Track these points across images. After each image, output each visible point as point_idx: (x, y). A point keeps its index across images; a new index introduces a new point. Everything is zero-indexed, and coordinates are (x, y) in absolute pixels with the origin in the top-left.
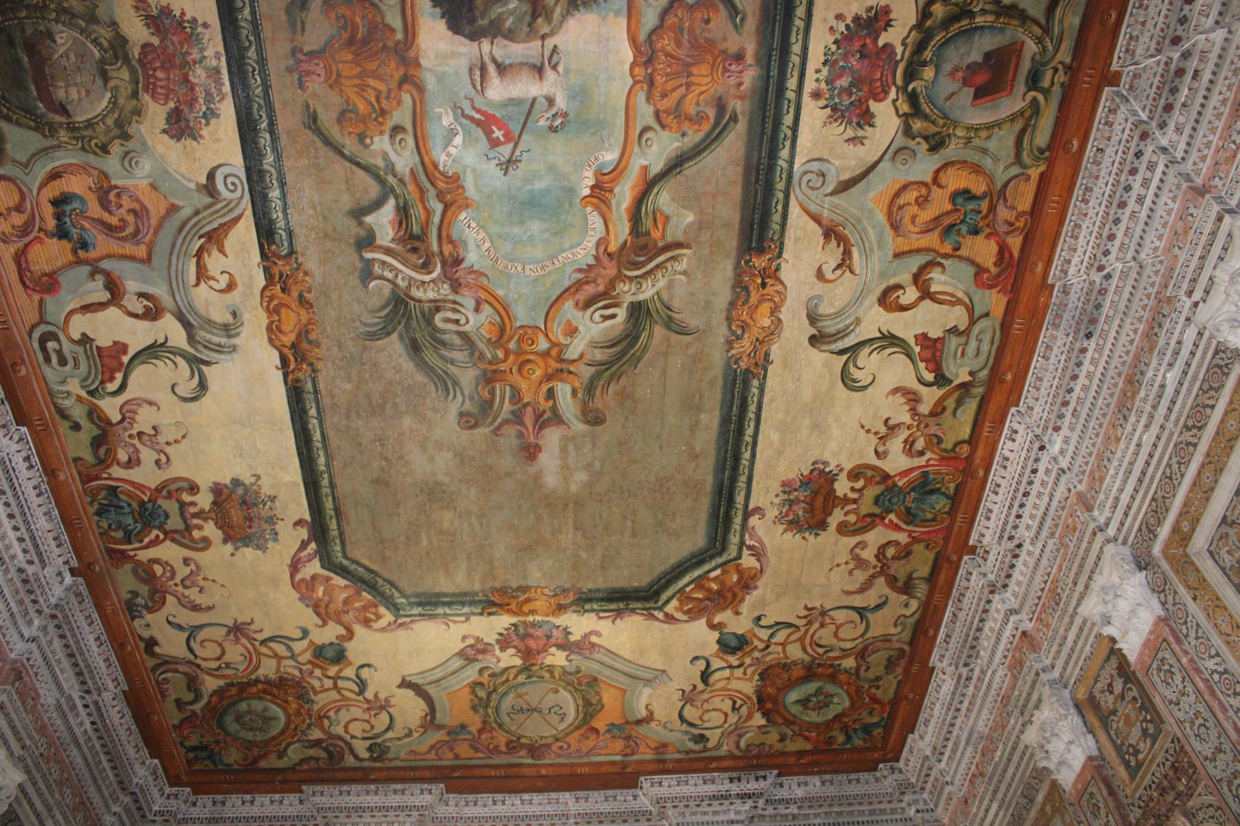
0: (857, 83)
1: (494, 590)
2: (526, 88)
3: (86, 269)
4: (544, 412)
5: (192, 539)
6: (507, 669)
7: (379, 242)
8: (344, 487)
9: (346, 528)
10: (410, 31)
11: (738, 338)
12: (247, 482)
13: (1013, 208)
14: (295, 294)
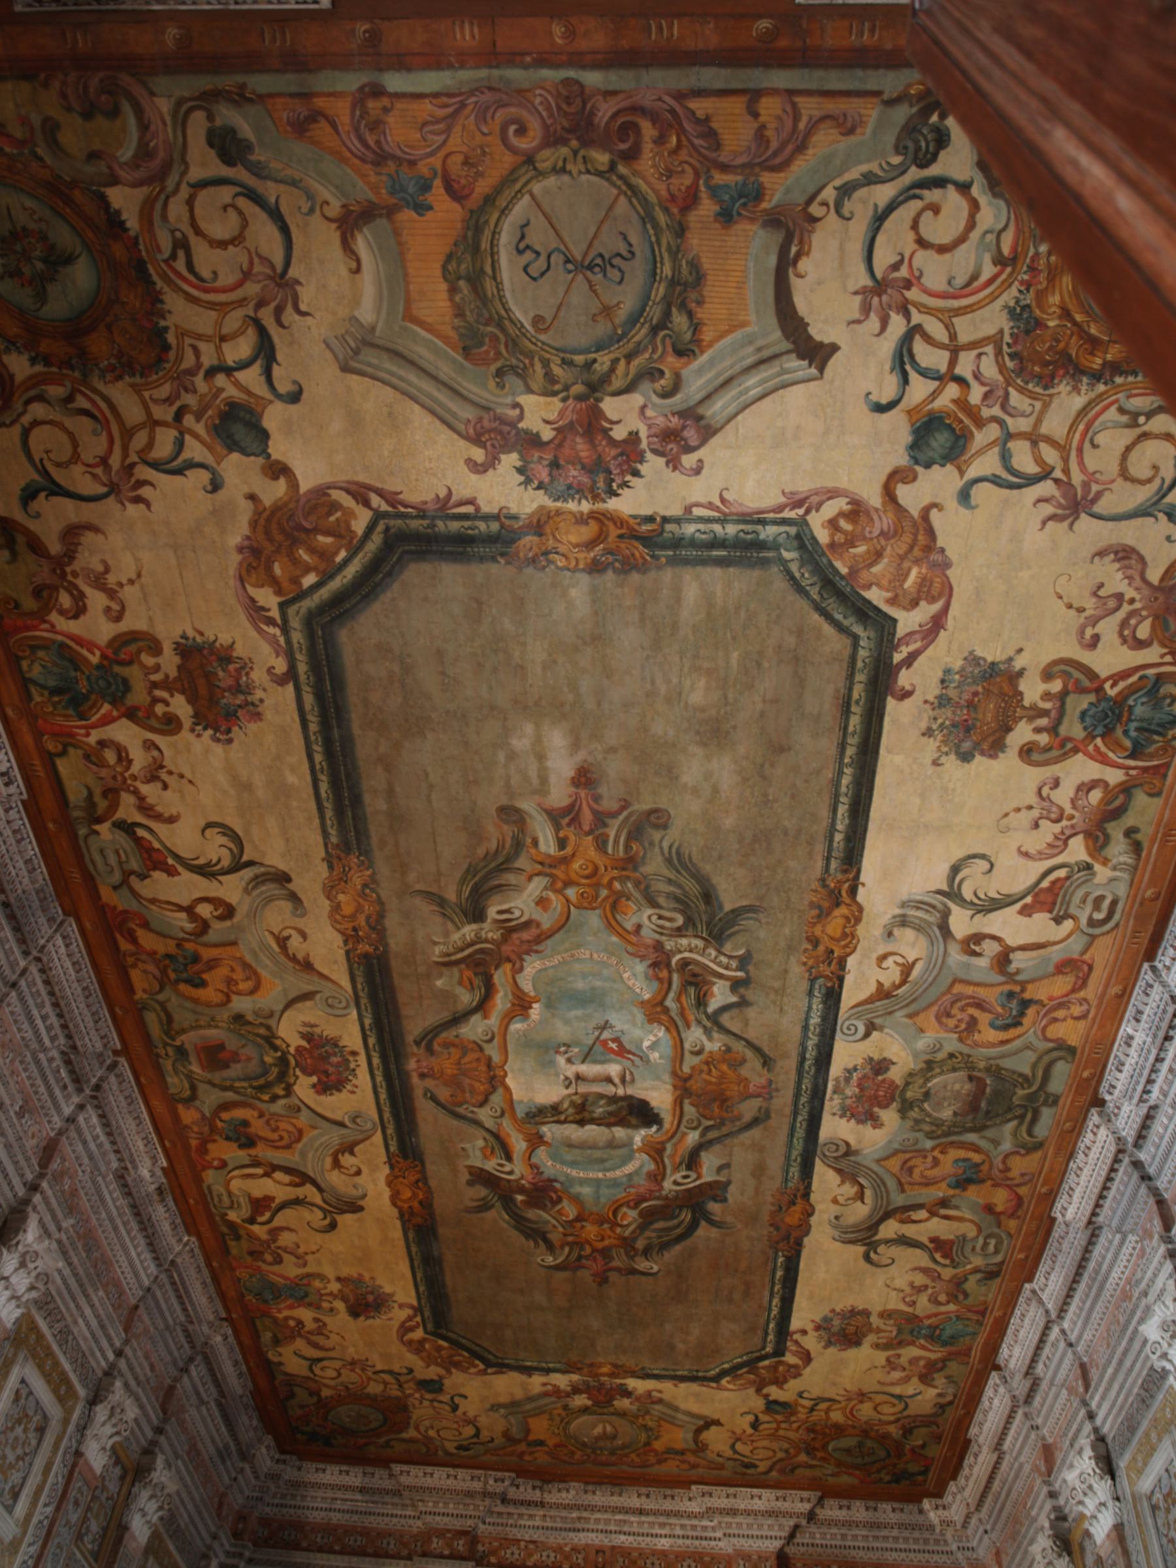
0: (324, 1058)
1: (642, 568)
3: (1019, 978)
4: (569, 825)
5: (1066, 675)
6: (629, 389)
7: (728, 984)
8: (828, 745)
9: (841, 684)
10: (678, 1103)
11: (365, 886)
12: (953, 757)
13: (145, 971)
14: (821, 948)
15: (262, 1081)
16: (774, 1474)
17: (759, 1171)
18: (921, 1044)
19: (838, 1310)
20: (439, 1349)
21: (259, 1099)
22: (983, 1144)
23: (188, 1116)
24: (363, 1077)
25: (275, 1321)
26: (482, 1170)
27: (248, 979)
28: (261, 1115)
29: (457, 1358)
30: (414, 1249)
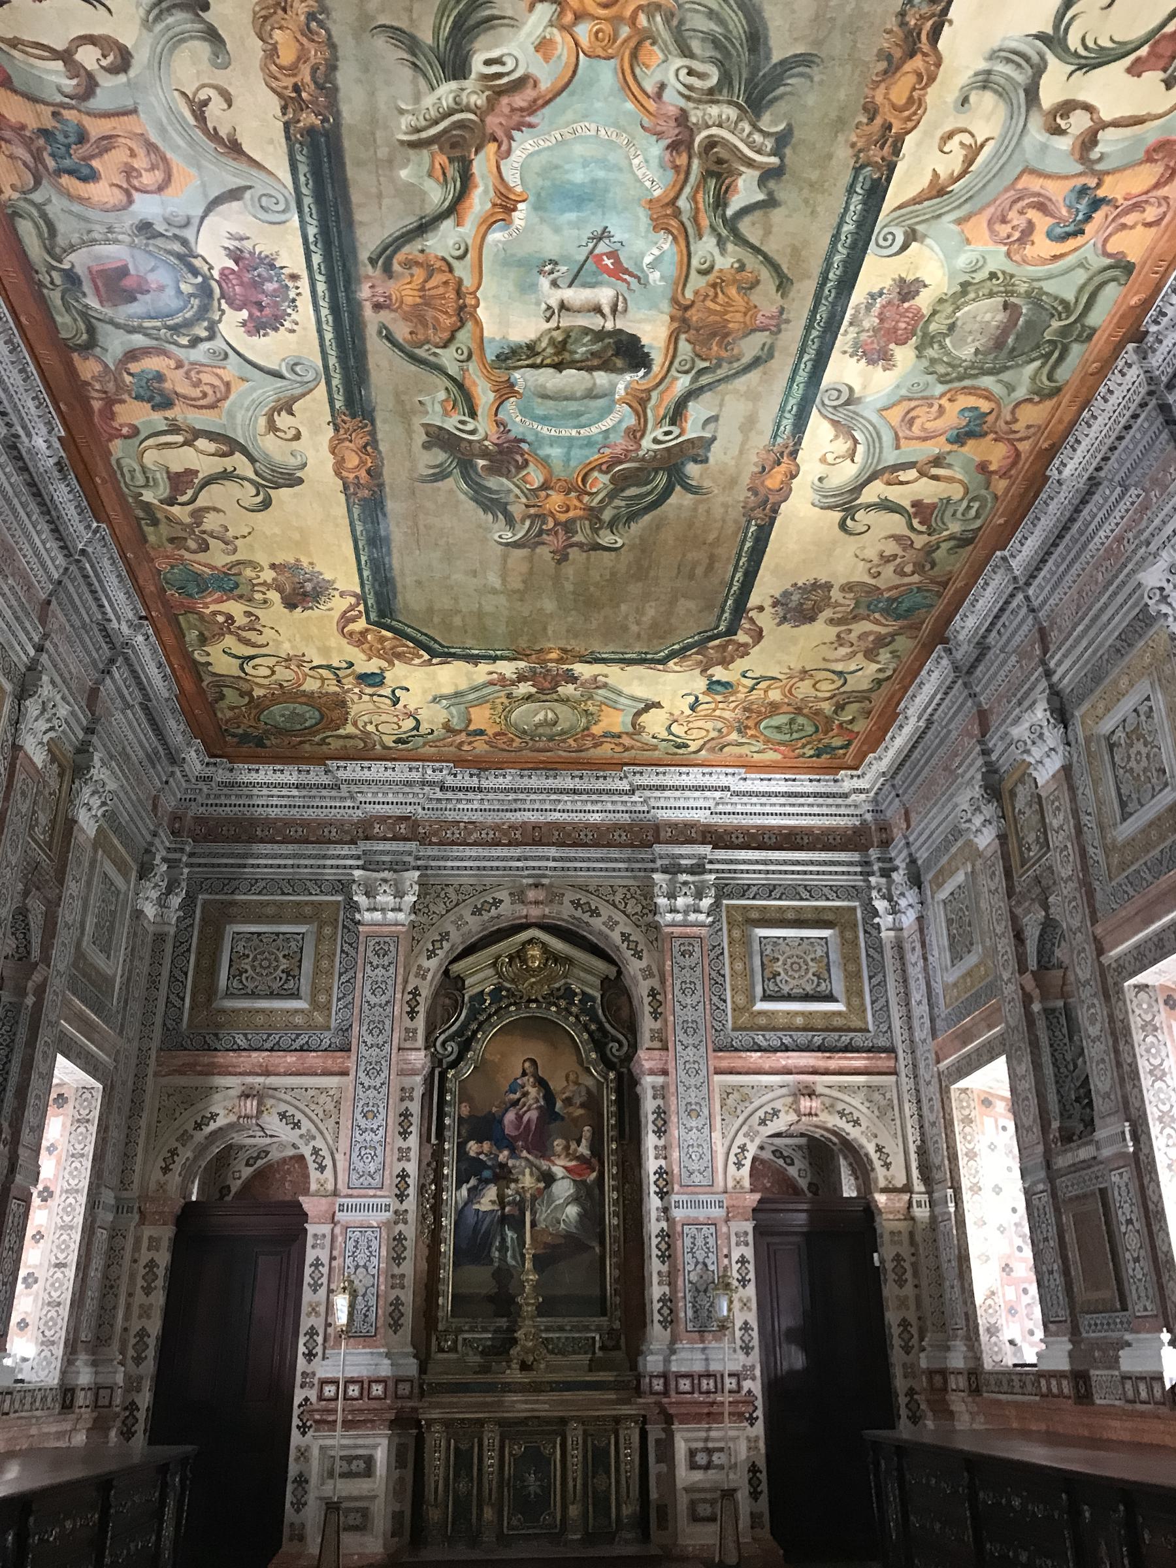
0: (256, 285)
2: (576, 295)
7: (757, 173)
10: (674, 338)
11: (311, 16)
14: (878, 121)
15: (178, 319)
16: (703, 752)
17: (749, 424)
18: (963, 261)
19: (800, 584)
20: (382, 640)
21: (176, 344)
22: (998, 390)
23: (88, 369)
24: (304, 313)
25: (201, 616)
26: (441, 428)
27: (153, 168)
28: (179, 366)
29: (400, 649)
30: (359, 528)
